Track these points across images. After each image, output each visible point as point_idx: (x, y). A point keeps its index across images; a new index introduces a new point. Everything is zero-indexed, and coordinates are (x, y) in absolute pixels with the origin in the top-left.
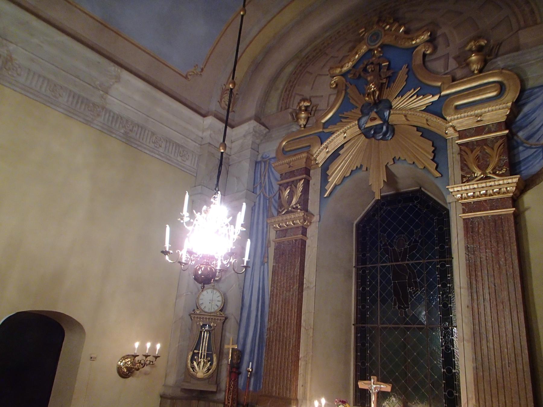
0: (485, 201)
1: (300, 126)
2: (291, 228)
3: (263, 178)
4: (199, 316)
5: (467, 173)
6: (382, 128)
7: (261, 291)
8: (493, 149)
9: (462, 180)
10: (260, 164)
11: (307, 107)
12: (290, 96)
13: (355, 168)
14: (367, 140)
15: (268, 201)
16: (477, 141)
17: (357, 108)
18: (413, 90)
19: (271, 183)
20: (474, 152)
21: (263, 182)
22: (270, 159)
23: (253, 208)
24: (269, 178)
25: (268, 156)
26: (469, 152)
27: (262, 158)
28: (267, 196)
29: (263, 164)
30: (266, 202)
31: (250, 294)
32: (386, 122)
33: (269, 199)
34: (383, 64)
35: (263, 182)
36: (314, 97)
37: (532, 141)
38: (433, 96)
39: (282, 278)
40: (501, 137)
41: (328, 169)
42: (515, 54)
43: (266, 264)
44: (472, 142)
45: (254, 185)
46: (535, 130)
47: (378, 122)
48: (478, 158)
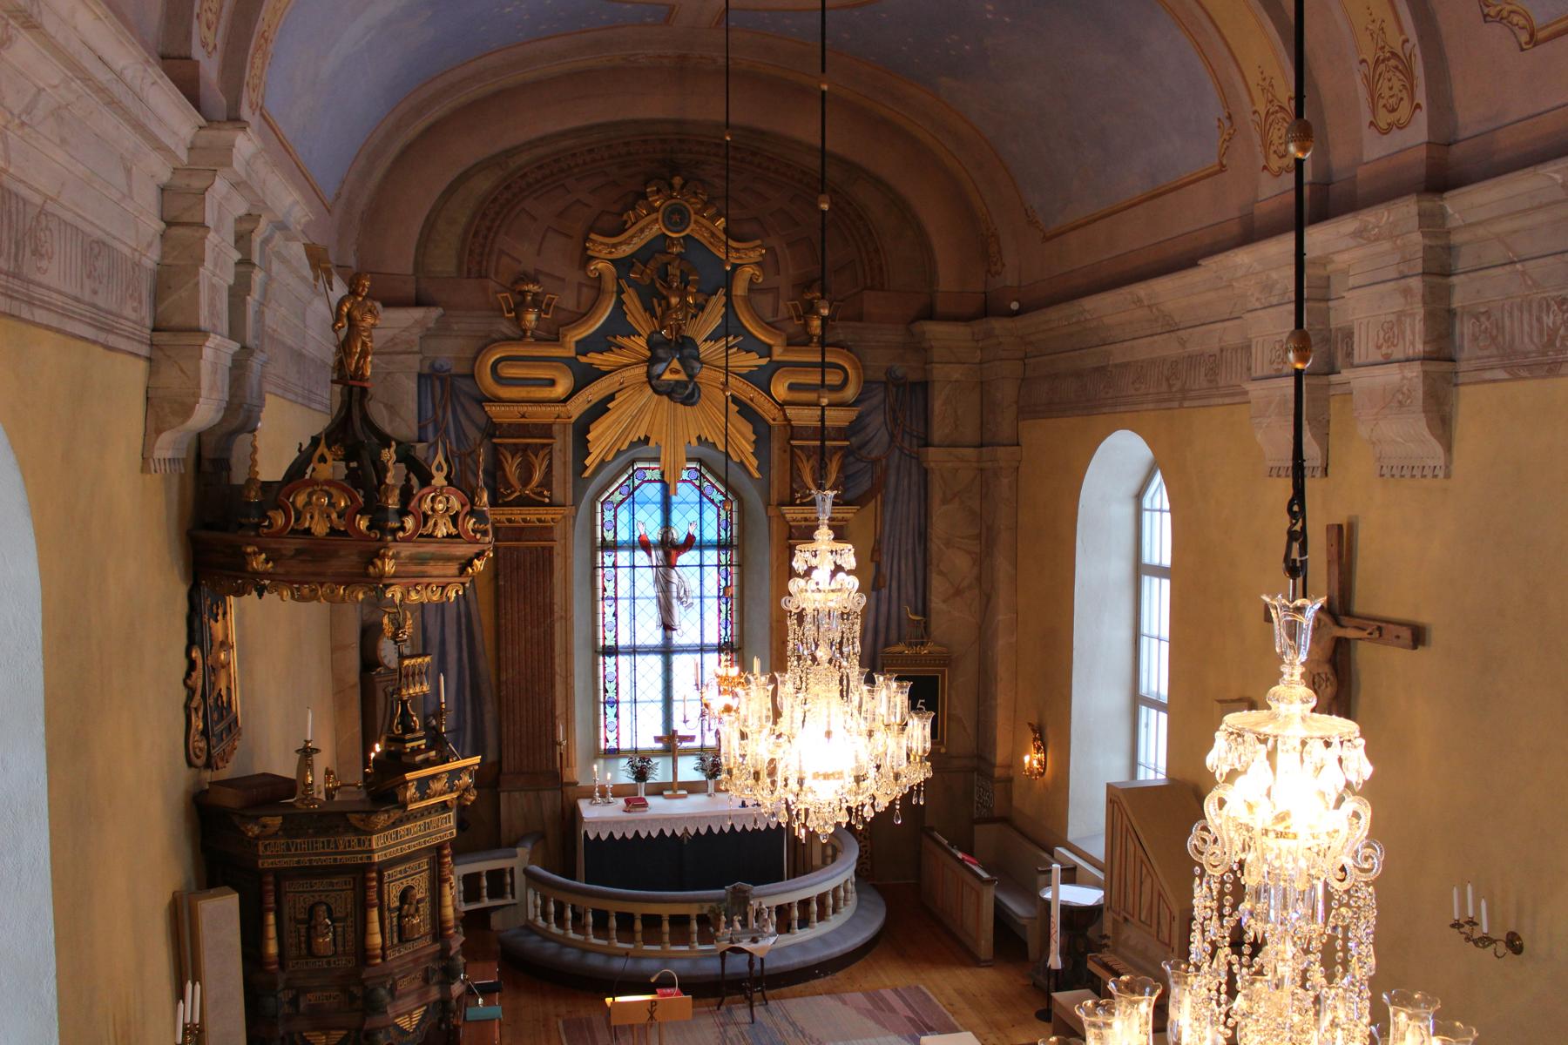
1: (525, 331)
3: (440, 413)
6: (687, 387)
7: (463, 620)
10: (429, 382)
11: (535, 294)
12: (487, 250)
13: (635, 440)
14: (656, 396)
17: (640, 335)
20: (811, 462)
21: (440, 419)
22: (451, 376)
25: (446, 368)
27: (432, 366)
29: (437, 384)
31: (439, 623)
32: (691, 377)
34: (690, 278)
36: (548, 275)
37: (864, 452)
40: (841, 448)
41: (589, 432)
42: (858, 324)
44: (808, 446)
45: (419, 422)
46: (867, 438)
47: (682, 377)
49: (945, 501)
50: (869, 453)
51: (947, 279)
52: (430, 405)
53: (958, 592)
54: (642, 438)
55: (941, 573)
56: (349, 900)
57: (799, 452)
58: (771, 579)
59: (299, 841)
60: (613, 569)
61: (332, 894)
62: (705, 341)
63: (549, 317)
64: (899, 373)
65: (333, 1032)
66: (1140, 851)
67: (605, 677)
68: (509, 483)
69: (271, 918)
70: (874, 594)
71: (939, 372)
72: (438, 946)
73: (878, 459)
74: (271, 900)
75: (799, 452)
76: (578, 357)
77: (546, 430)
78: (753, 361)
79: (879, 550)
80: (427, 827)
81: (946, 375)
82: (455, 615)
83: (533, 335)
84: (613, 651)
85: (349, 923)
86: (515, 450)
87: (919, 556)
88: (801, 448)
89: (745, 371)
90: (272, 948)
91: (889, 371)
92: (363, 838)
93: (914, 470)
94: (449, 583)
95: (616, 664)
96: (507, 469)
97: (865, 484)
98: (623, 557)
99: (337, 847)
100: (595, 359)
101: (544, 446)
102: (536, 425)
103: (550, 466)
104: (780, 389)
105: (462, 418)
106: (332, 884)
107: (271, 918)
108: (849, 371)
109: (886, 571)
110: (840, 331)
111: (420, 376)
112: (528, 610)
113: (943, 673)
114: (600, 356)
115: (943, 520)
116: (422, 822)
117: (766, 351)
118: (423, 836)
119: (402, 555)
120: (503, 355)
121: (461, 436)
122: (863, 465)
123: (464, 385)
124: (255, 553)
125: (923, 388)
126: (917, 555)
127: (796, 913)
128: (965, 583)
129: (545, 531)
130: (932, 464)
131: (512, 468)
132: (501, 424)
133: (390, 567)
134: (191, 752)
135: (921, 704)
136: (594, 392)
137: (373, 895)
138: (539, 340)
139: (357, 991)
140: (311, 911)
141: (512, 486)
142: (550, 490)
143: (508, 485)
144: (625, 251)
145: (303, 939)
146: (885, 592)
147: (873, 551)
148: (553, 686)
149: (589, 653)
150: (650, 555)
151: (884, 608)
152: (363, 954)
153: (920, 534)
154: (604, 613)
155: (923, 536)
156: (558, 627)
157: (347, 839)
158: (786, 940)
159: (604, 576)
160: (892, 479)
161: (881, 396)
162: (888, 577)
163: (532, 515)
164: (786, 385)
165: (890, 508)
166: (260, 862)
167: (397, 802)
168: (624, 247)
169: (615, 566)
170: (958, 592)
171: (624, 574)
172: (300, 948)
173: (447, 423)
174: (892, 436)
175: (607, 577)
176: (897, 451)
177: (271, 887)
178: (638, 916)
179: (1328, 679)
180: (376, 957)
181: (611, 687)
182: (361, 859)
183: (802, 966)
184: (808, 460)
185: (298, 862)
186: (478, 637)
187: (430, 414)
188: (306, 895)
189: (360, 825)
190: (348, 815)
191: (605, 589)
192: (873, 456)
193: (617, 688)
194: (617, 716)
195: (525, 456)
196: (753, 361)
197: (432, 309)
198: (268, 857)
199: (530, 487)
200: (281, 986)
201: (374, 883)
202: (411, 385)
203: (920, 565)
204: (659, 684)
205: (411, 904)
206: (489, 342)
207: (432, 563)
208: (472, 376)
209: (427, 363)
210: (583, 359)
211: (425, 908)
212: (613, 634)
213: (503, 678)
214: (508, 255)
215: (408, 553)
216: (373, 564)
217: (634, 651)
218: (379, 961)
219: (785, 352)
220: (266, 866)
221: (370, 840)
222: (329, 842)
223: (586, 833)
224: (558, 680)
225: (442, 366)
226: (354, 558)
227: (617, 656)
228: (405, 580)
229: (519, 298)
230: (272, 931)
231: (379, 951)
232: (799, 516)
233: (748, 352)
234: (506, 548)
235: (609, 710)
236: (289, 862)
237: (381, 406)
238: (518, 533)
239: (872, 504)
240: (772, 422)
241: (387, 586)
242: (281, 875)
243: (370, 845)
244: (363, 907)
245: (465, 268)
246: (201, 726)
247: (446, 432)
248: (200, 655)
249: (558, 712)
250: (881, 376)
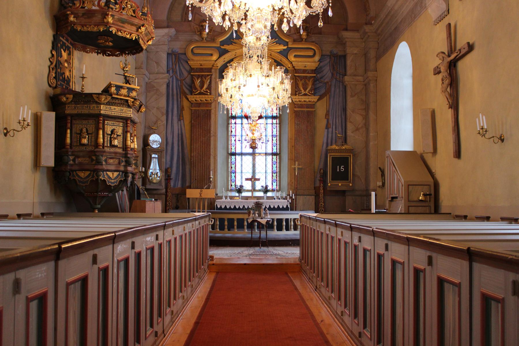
0: (304, 104)
1: (203, 38)
2: (204, 103)
3: (174, 66)
4: (151, 150)
5: (298, 90)
7: (180, 136)
8: (309, 81)
9: (296, 93)
10: (171, 56)
15: (179, 82)
16: (303, 76)
18: (274, 39)
19: (181, 70)
20: (302, 81)
21: (174, 68)
23: (168, 85)
24: (179, 67)
25: (177, 51)
26: (300, 81)
27: (172, 51)
28: (179, 78)
29: (174, 56)
30: (178, 83)
31: (172, 137)
33: (180, 81)
35: (174, 68)
37: (322, 80)
38: (284, 46)
39: (199, 130)
40: (313, 77)
41: (224, 72)
43: (182, 121)
45: (167, 69)
46: (324, 75)
48: (303, 85)
49: (352, 96)
50: (324, 80)
51: (351, 19)
52: (171, 64)
53: (357, 129)
55: (351, 122)
56: (93, 128)
57: (297, 78)
58: (288, 124)
59: (78, 106)
60: (235, 125)
61: (89, 125)
63: (211, 33)
64: (335, 52)
65: (86, 172)
66: (394, 168)
67: (231, 162)
68: (196, 88)
69: (69, 131)
70: (326, 130)
71: (349, 50)
72: (124, 152)
73: (327, 82)
74: (69, 125)
75: (297, 78)
76: (221, 47)
77: (209, 70)
78: (282, 47)
79: (328, 115)
80: (122, 110)
81: (352, 51)
82: (177, 135)
83: (205, 40)
84: (234, 154)
85: (93, 135)
86: (198, 77)
87: (343, 117)
88: (299, 76)
89: (279, 51)
90: (68, 141)
91: (331, 52)
92: (98, 105)
93: (341, 86)
94: (133, 33)
95: (235, 158)
96: (196, 83)
97: (323, 91)
98: (239, 121)
99: (90, 108)
100: (226, 47)
101: (208, 75)
102: (206, 69)
103: (210, 82)
104: (291, 58)
105: (182, 68)
106: (88, 122)
107: (69, 131)
108: (316, 50)
109: (331, 122)
110: (313, 38)
111: (168, 54)
112: (202, 132)
113: (350, 156)
114: (228, 46)
115: (352, 103)
116: (120, 108)
117: (286, 44)
118: (119, 112)
119: (116, 17)
120: (195, 46)
121: (181, 73)
122: (322, 84)
123: (183, 57)
124: (70, 14)
125: (344, 57)
126: (342, 116)
127: (284, 223)
128: (360, 126)
129: (209, 104)
130: (346, 82)
131: (198, 82)
132: (194, 69)
133: (110, 20)
134: (49, 81)
135: (343, 167)
136: (227, 57)
137: (101, 126)
138: (207, 41)
139: (94, 158)
140: (81, 130)
141: (197, 89)
142: (210, 90)
143: (196, 89)
145: (78, 139)
146: (330, 130)
147: (326, 115)
148: (209, 158)
149: (225, 154)
150: (248, 120)
151: (330, 135)
152: (97, 145)
153: (343, 109)
154: (231, 140)
155: (345, 110)
156: (212, 138)
157: (93, 105)
158: (280, 233)
159: (231, 127)
160: (333, 89)
161: (328, 60)
162: (332, 125)
163: (203, 98)
164: (293, 55)
165: (332, 99)
166: (66, 111)
167: (109, 93)
169: (235, 123)
170: (357, 129)
171: (239, 127)
172: (77, 143)
173: (177, 69)
174: (333, 74)
175: (233, 127)
176: (334, 79)
177: (69, 121)
178: (226, 219)
179: (446, 77)
180: (100, 146)
181: (233, 166)
182: (97, 112)
183: (284, 239)
184: (301, 81)
185: (78, 112)
186: (185, 142)
187: (171, 66)
188: (80, 125)
189: (97, 99)
190: (93, 95)
191: (232, 132)
192: (326, 81)
193: (235, 167)
194: (235, 177)
195: (202, 79)
196: (282, 47)
197: (171, 29)
198: (68, 110)
199: (203, 89)
200: (70, 153)
201: (101, 122)
202: (165, 56)
203: (344, 121)
204: (251, 166)
205: (115, 134)
206: (191, 42)
207: (126, 24)
208: (185, 54)
209: (170, 50)
210: (222, 47)
211: (121, 138)
212: (234, 147)
213: (192, 155)
214: (198, 14)
215: (117, 17)
216: (105, 18)
217: (242, 154)
218: (101, 147)
219: (292, 44)
220: (68, 113)
221: (100, 106)
222: (88, 106)
223: (217, 205)
224: (212, 157)
225: (175, 51)
226: (100, 16)
227: (235, 156)
228: (117, 27)
229: (201, 28)
230: (69, 135)
231: (101, 144)
232: (297, 100)
233: (279, 44)
234: (194, 110)
235: (232, 174)
236: (75, 112)
237: (154, 62)
238: (199, 105)
239: (325, 98)
240: (288, 69)
241: (110, 27)
242: (72, 116)
243: (100, 108)
244: (98, 129)
245: (184, 19)
246: (54, 76)
247: (176, 72)
248: (55, 54)
249: (211, 169)
250: (328, 53)
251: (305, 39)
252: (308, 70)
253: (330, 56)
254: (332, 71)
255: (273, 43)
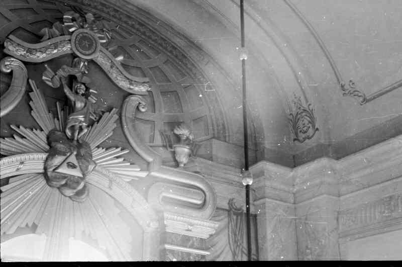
6: (78, 183)
18: (119, 149)
34: (91, 91)
54: (30, 225)
62: (98, 147)
144: (40, 57)
168: (38, 54)
250: (227, 208)
251: (185, 165)
252: (192, 237)
253: (229, 211)
254: (232, 247)
255: (117, 157)
